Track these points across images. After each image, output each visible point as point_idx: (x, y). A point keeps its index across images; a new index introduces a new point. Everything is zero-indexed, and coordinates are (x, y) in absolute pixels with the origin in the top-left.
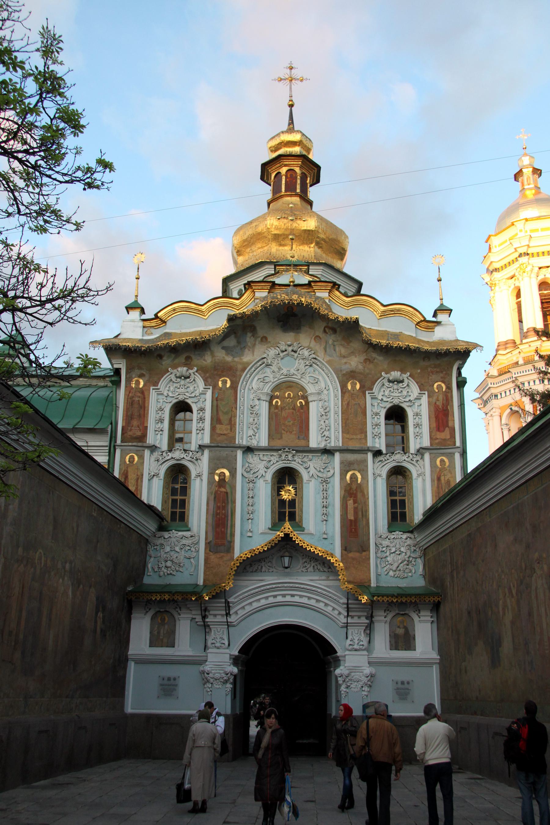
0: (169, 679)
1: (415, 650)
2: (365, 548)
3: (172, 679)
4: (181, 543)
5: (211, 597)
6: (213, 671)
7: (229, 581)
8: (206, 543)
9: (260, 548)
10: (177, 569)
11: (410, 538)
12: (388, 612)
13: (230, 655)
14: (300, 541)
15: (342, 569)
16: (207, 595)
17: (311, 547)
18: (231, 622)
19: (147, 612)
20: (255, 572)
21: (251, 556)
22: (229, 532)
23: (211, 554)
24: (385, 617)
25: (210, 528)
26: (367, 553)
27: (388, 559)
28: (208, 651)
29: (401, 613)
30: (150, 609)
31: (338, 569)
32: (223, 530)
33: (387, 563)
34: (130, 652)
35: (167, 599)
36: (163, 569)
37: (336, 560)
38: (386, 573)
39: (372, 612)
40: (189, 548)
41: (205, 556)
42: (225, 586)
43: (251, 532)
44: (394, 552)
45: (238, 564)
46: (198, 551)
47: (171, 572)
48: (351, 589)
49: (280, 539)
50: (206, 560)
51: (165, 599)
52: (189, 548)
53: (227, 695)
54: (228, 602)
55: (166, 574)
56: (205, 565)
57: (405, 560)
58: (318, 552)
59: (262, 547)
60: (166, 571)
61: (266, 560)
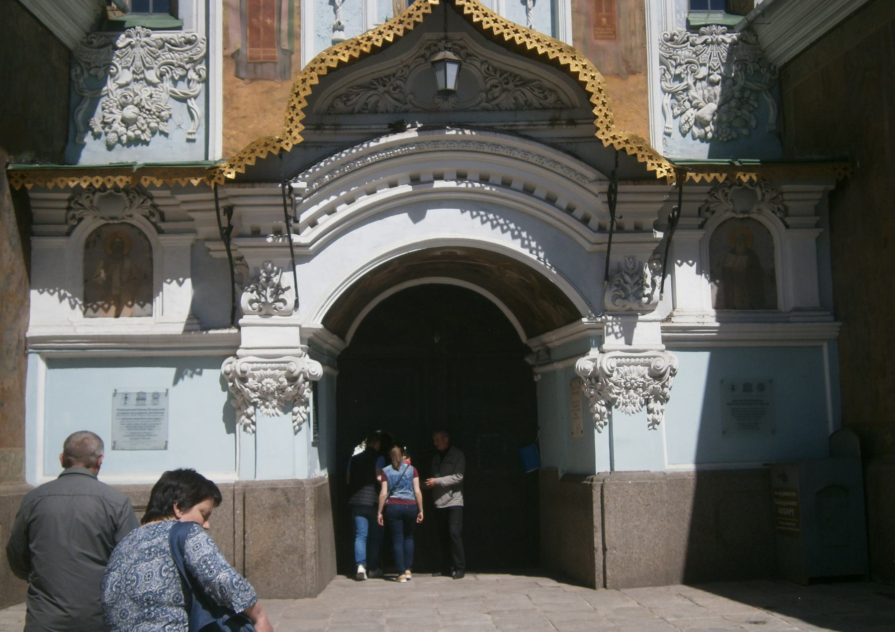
0: (141, 397)
1: (775, 307)
2: (632, 67)
3: (149, 398)
4: (161, 61)
5: (242, 171)
6: (256, 373)
7: (292, 126)
8: (225, 57)
9: (375, 37)
10: (153, 125)
11: (745, 42)
12: (708, 214)
13: (302, 330)
14: (486, 15)
15: (600, 91)
16: (232, 166)
17: (516, 32)
18: (300, 246)
19: (74, 227)
20: (359, 112)
21: (351, 56)
22: (284, 26)
23: (241, 83)
24: (701, 227)
25: (235, 20)
26: (641, 77)
27: (692, 93)
28: (241, 321)
29: (741, 216)
30: (80, 220)
31: (589, 88)
32: (269, 21)
33: (687, 104)
34: (32, 332)
35: (121, 185)
36: (115, 126)
37: (584, 67)
38: (687, 127)
39: (678, 210)
40: (180, 72)
41: (224, 89)
42: (280, 141)
43: (341, 29)
44: (703, 79)
45: (316, 81)
46: (206, 81)
47: (138, 132)
48: (627, 142)
49: (429, 11)
50: (229, 99)
51: (116, 188)
52: (180, 72)
53: (296, 433)
54: (291, 189)
55: (124, 138)
56: (225, 113)
57: (733, 97)
58: (535, 44)
59: (380, 33)
60: (123, 129)
61: (388, 85)
